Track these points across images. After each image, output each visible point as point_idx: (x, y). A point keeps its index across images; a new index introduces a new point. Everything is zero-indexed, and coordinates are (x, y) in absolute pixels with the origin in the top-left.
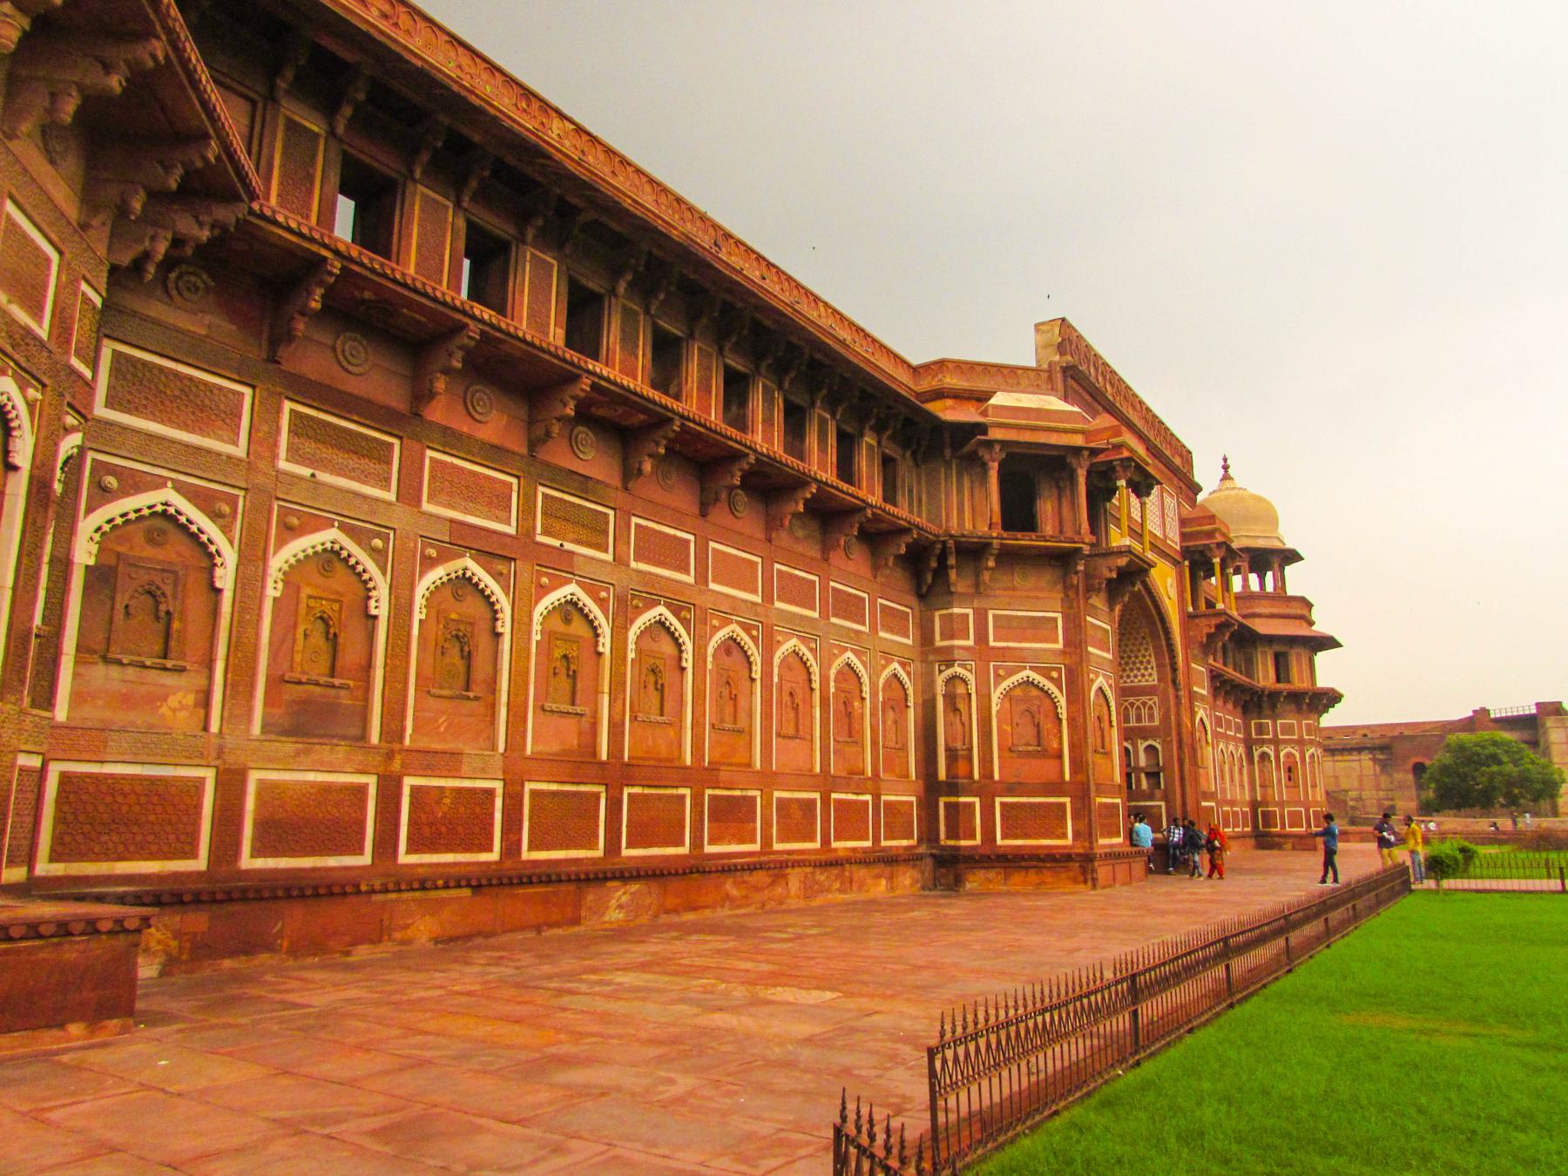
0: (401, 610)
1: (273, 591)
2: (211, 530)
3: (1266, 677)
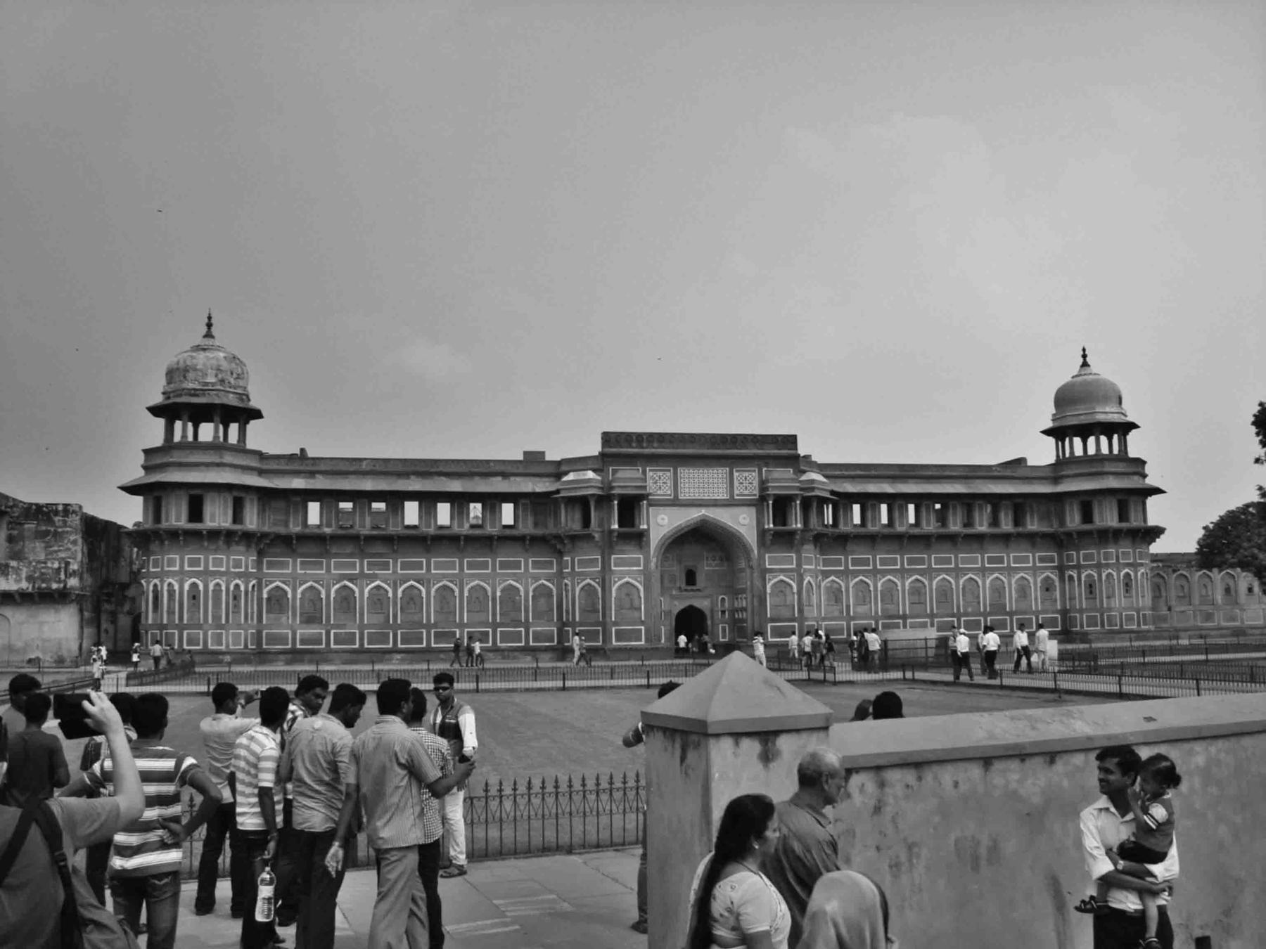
0: (328, 596)
1: (299, 596)
2: (286, 587)
3: (1072, 521)
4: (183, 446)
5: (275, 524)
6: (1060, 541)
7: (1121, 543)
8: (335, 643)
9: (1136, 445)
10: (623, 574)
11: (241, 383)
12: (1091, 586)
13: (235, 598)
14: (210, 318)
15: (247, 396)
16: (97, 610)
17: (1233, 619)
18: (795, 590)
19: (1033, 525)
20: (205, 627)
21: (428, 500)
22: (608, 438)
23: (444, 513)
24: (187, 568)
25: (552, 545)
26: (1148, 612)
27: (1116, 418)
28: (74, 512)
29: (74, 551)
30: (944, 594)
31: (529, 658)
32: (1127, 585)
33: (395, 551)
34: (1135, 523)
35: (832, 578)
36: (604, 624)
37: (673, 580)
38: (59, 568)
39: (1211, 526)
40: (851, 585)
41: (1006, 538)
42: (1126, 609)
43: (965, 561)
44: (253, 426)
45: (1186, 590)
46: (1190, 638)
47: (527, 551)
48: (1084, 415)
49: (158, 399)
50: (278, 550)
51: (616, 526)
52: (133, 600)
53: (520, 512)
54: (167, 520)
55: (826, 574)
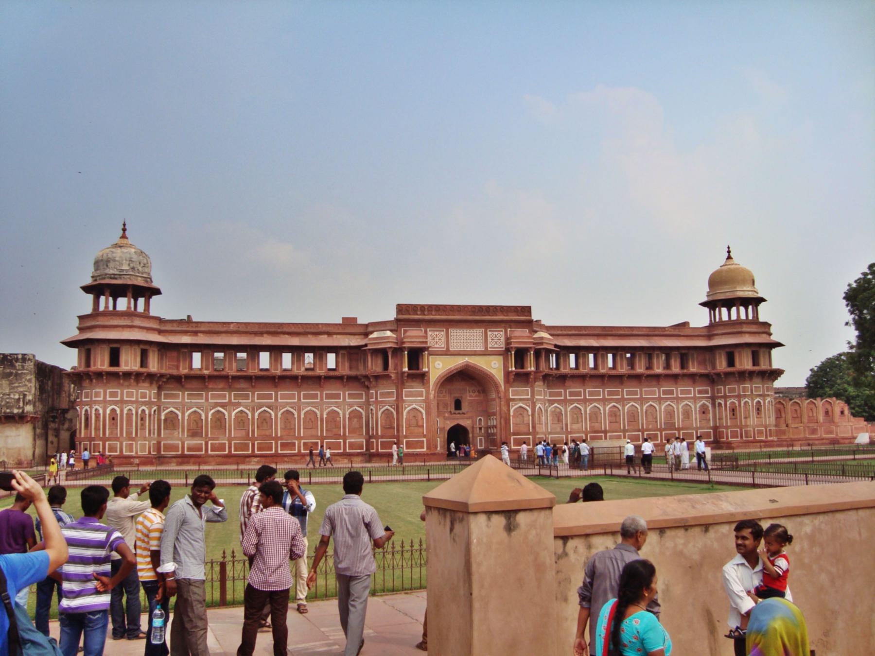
0: (207, 417)
1: (186, 418)
4: (106, 314)
5: (169, 368)
6: (712, 379)
7: (755, 380)
8: (212, 451)
9: (764, 313)
11: (146, 270)
12: (733, 410)
13: (142, 419)
14: (124, 225)
15: (151, 279)
16: (45, 427)
17: (831, 432)
18: (530, 413)
19: (693, 368)
20: (121, 439)
21: (276, 351)
22: (400, 308)
23: (287, 360)
24: (108, 399)
25: (361, 382)
26: (773, 428)
27: (751, 295)
28: (29, 359)
29: (29, 386)
30: (633, 417)
31: (346, 461)
32: (758, 410)
33: (253, 387)
34: (763, 366)
36: (398, 437)
37: (446, 406)
38: (19, 399)
39: (816, 369)
40: (569, 409)
41: (675, 377)
42: (758, 426)
43: (647, 393)
44: (154, 299)
45: (799, 411)
46: (801, 446)
47: (344, 386)
48: (729, 294)
49: (88, 281)
50: (172, 386)
51: (406, 369)
52: (71, 420)
53: (340, 360)
54: (95, 365)
55: (551, 402)
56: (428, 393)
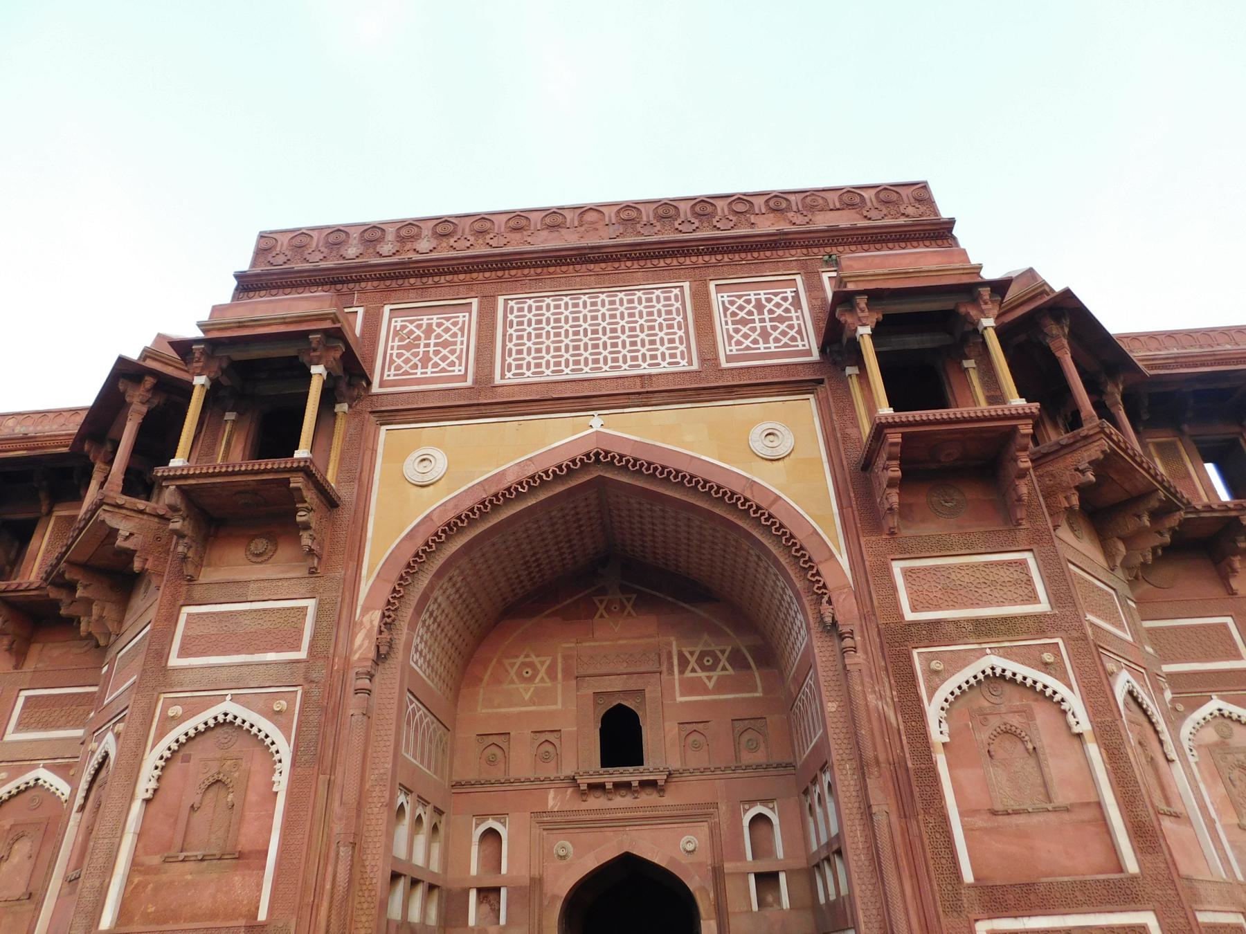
10: (216, 683)
18: (1083, 724)
35: (1215, 704)
56: (334, 620)
